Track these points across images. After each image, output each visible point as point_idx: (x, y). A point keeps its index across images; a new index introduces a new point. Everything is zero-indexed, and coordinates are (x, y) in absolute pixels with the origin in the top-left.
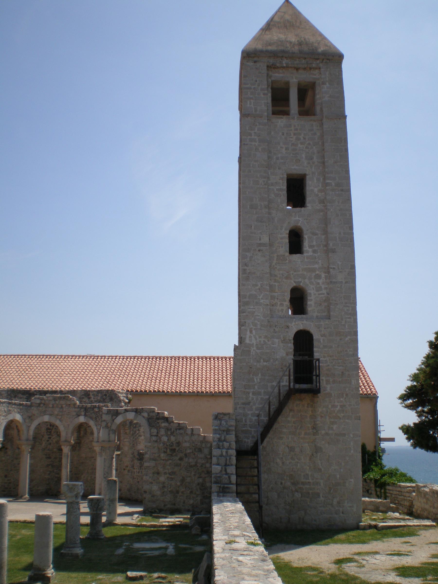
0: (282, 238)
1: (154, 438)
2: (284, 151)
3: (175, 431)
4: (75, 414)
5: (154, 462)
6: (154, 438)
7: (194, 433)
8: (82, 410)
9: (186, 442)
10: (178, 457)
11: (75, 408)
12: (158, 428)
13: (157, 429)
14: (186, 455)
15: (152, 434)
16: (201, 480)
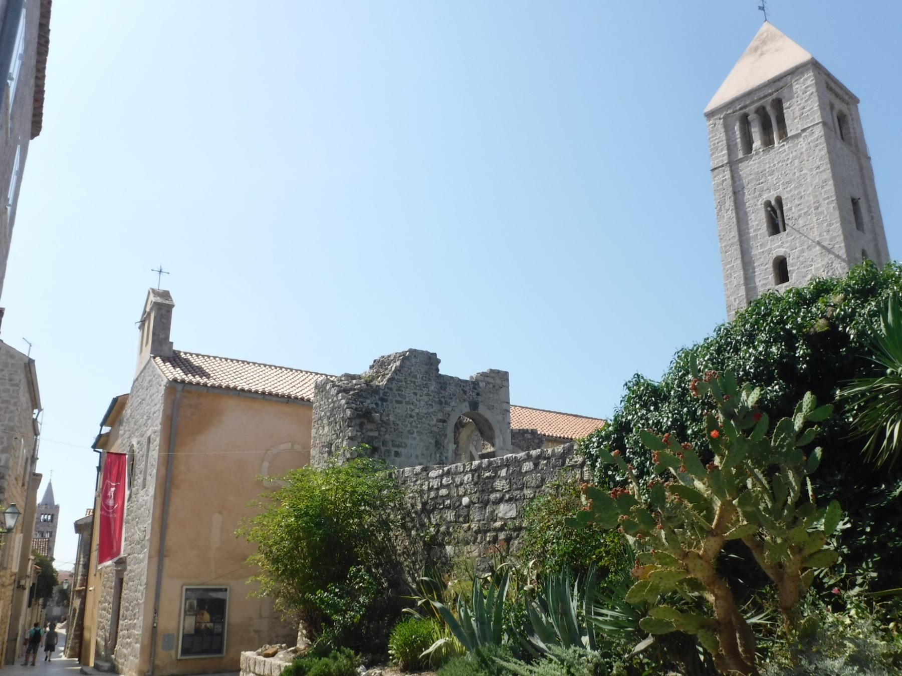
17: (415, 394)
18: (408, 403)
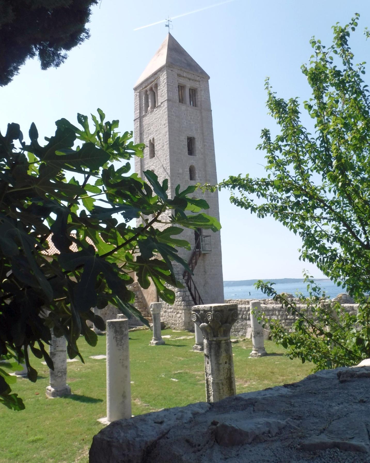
0: (187, 171)
2: (185, 123)
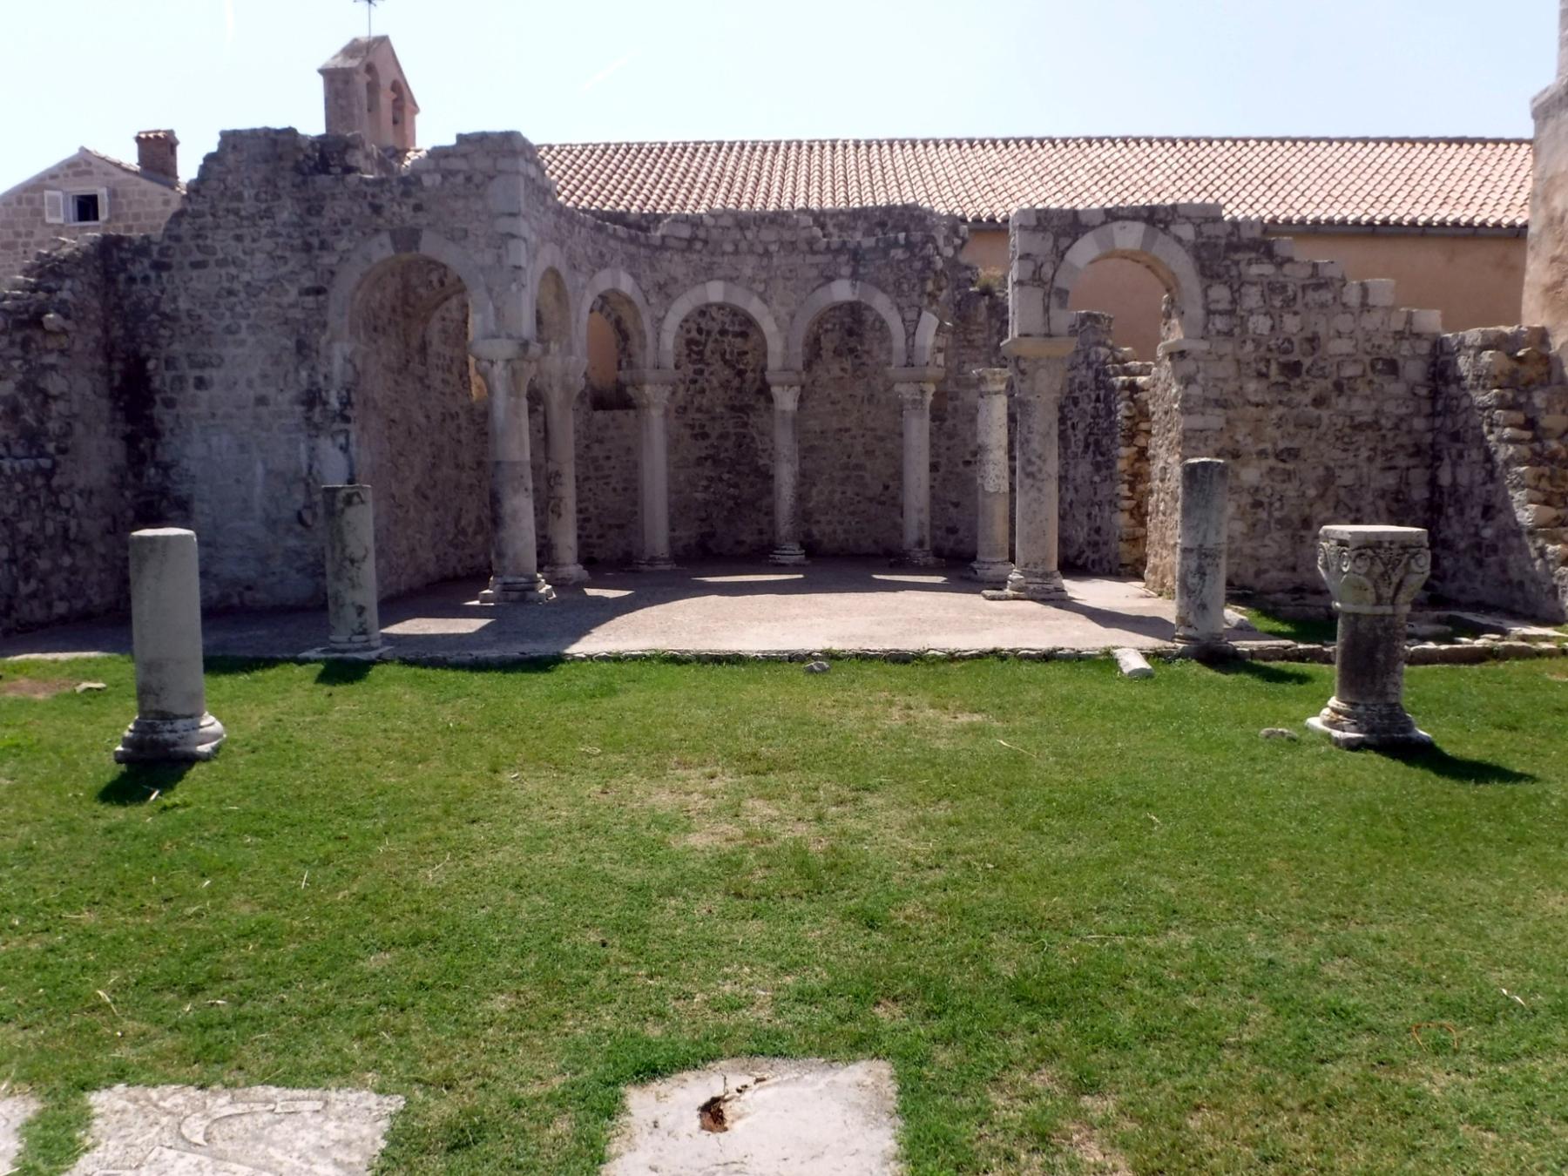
1: (1220, 323)
3: (1300, 295)
4: (814, 273)
5: (1219, 411)
6: (1220, 323)
7: (1371, 301)
8: (843, 258)
9: (1339, 335)
10: (1312, 393)
11: (814, 252)
12: (1237, 287)
13: (1231, 287)
14: (1339, 387)
15: (1212, 307)
16: (1390, 480)
17: (239, 238)
18: (222, 263)
